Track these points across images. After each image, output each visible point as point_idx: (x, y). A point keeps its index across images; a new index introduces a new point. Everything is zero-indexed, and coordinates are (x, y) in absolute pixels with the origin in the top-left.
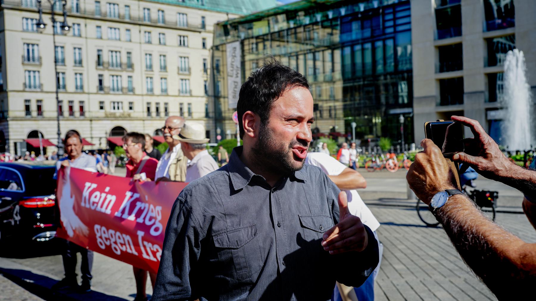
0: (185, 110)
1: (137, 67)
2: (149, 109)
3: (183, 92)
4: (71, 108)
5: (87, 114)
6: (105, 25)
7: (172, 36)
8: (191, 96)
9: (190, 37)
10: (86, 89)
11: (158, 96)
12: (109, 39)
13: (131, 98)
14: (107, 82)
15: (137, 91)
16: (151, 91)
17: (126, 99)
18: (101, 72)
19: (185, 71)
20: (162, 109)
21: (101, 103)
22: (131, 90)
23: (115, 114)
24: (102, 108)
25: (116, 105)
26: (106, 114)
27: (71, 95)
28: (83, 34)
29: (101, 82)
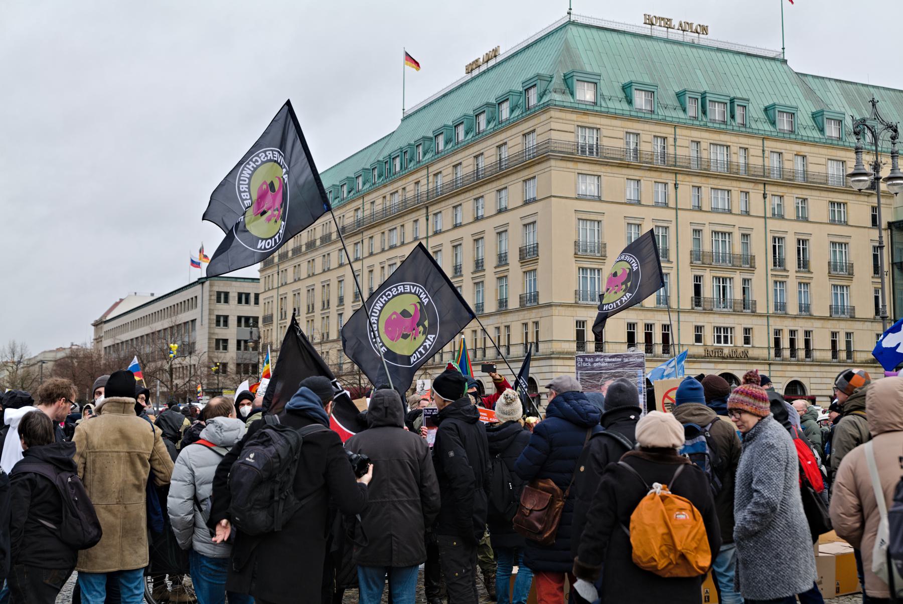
0: (841, 345)
1: (760, 263)
2: (777, 342)
3: (837, 312)
4: (648, 337)
5: (675, 350)
6: (707, 185)
7: (818, 205)
8: (853, 318)
9: (850, 206)
10: (674, 305)
11: (795, 317)
12: (715, 210)
13: (747, 322)
14: (709, 291)
15: (760, 309)
16: (781, 307)
17: (738, 323)
18: (699, 273)
19: (841, 272)
20: (800, 344)
21: (698, 328)
22: (747, 306)
23: (721, 349)
24: (698, 339)
25: (723, 334)
26: (706, 350)
27: (649, 314)
28: (672, 204)
29: (697, 289)
